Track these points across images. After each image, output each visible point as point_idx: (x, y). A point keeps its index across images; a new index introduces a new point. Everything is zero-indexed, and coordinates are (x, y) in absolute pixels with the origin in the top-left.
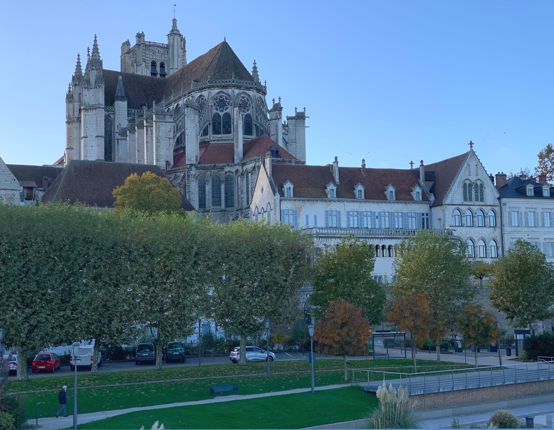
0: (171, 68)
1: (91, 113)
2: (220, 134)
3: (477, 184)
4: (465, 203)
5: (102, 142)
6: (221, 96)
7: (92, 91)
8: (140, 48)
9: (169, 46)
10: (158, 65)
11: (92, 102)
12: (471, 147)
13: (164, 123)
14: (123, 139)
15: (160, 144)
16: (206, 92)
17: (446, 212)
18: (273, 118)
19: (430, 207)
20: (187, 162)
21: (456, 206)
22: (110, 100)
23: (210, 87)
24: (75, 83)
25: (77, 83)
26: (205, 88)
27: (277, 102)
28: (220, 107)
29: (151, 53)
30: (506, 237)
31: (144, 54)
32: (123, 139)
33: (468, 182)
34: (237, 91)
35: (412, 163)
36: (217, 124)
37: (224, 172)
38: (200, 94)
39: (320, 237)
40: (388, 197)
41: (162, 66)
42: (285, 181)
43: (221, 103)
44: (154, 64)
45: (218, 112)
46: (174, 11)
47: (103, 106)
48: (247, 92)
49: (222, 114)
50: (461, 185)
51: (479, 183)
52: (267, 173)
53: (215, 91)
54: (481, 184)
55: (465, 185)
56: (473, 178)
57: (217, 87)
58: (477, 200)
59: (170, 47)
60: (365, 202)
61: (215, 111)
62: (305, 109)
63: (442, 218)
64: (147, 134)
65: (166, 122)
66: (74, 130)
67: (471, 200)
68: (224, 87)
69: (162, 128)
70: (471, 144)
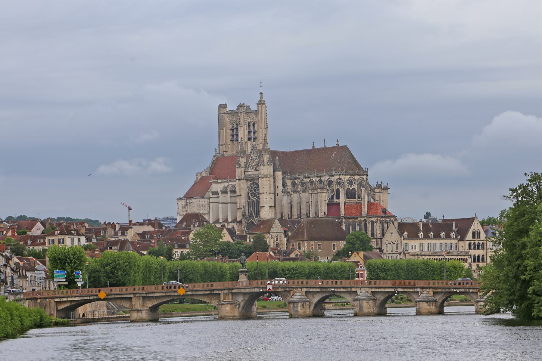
0: (260, 127)
1: (265, 179)
2: (350, 199)
3: (477, 232)
4: (473, 240)
5: (272, 196)
6: (351, 179)
7: (265, 167)
8: (241, 114)
9: (259, 112)
10: (252, 125)
11: (266, 173)
12: (476, 215)
13: (323, 193)
14: (285, 195)
15: (322, 204)
16: (343, 176)
17: (466, 244)
18: (377, 192)
19: (458, 241)
20: (341, 215)
21: (470, 241)
22: (274, 171)
23: (345, 175)
24: (242, 156)
25: (243, 156)
26: (342, 175)
27: (379, 183)
28: (350, 185)
29: (248, 117)
30: (488, 254)
31: (245, 119)
32: (285, 195)
33: (474, 231)
34: (358, 177)
35: (443, 216)
36: (348, 193)
37: (358, 220)
38: (339, 177)
39: (422, 256)
40: (442, 237)
41: (254, 124)
42: (404, 231)
43: (351, 183)
44: (249, 124)
45: (349, 187)
46: (261, 86)
47: (273, 176)
48: (363, 177)
49: (351, 188)
50: (472, 232)
51: (478, 231)
52: (395, 227)
53: (347, 177)
54: (479, 232)
55: (473, 232)
56: (476, 229)
57: (349, 174)
58: (477, 238)
59: (259, 113)
60: (434, 239)
61: (348, 187)
62: (387, 184)
63: (464, 246)
64: (311, 197)
65: (324, 192)
66: (242, 184)
67: (475, 238)
68: (352, 175)
69: (323, 196)
70: (476, 214)
